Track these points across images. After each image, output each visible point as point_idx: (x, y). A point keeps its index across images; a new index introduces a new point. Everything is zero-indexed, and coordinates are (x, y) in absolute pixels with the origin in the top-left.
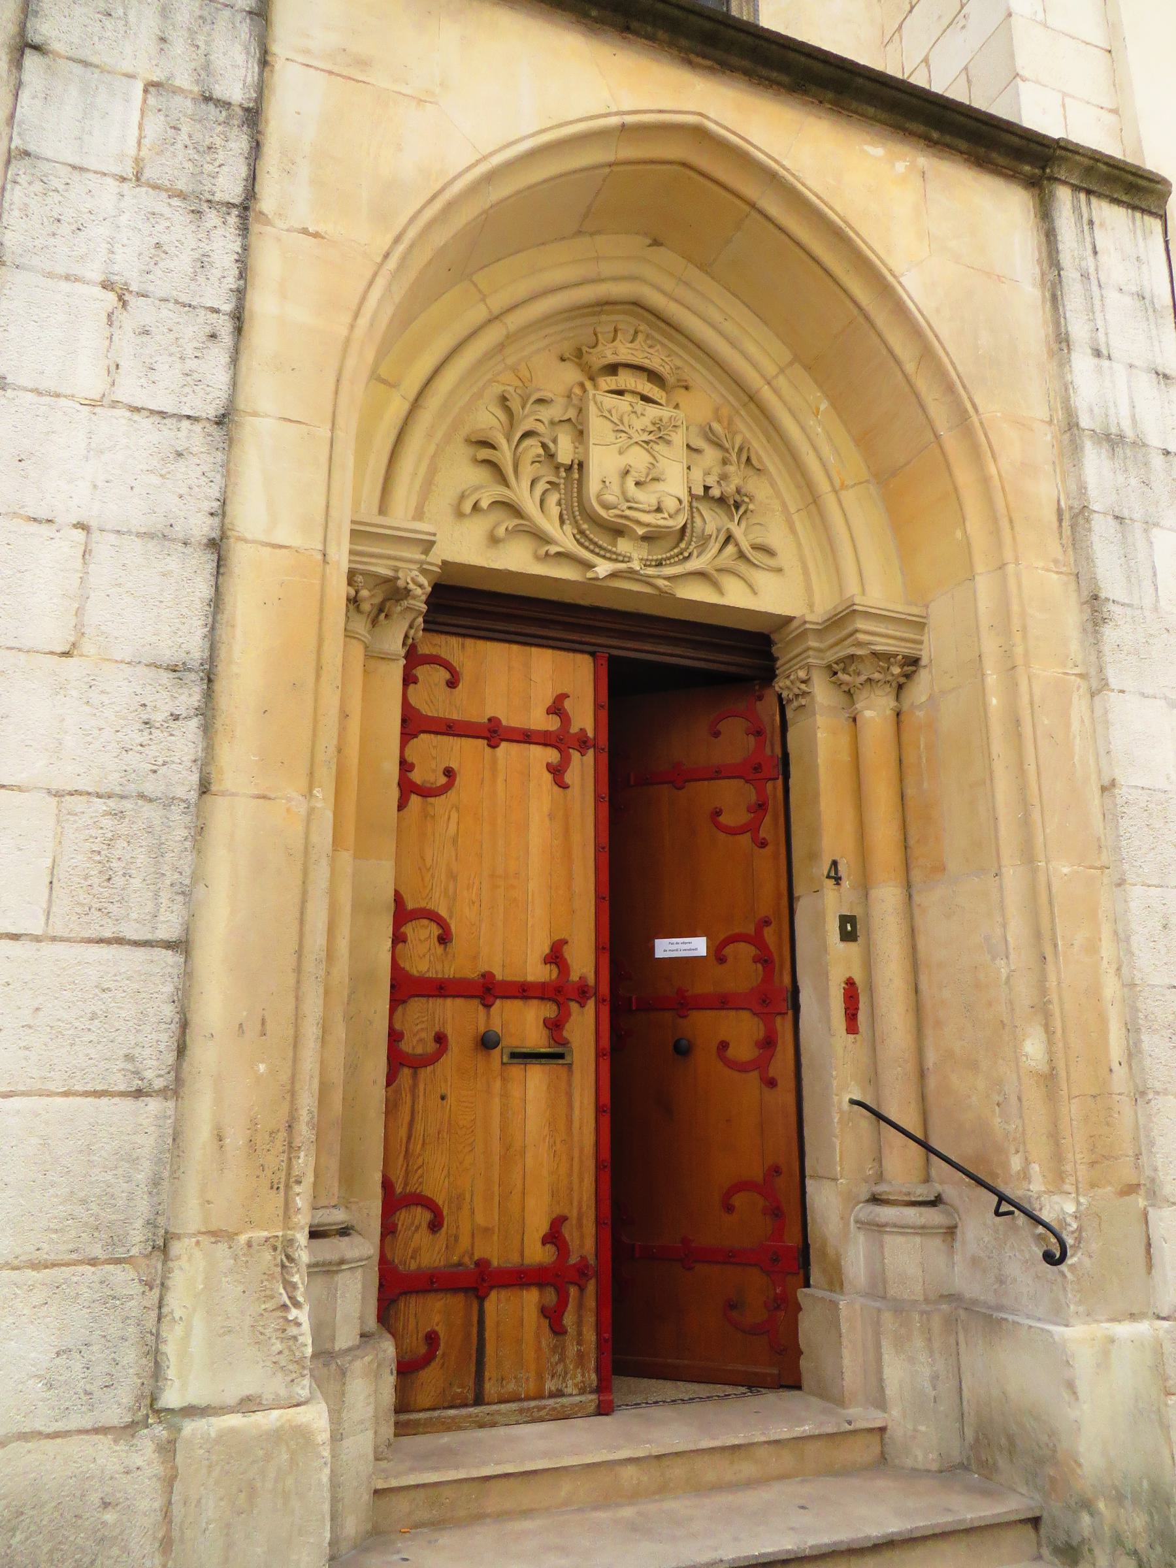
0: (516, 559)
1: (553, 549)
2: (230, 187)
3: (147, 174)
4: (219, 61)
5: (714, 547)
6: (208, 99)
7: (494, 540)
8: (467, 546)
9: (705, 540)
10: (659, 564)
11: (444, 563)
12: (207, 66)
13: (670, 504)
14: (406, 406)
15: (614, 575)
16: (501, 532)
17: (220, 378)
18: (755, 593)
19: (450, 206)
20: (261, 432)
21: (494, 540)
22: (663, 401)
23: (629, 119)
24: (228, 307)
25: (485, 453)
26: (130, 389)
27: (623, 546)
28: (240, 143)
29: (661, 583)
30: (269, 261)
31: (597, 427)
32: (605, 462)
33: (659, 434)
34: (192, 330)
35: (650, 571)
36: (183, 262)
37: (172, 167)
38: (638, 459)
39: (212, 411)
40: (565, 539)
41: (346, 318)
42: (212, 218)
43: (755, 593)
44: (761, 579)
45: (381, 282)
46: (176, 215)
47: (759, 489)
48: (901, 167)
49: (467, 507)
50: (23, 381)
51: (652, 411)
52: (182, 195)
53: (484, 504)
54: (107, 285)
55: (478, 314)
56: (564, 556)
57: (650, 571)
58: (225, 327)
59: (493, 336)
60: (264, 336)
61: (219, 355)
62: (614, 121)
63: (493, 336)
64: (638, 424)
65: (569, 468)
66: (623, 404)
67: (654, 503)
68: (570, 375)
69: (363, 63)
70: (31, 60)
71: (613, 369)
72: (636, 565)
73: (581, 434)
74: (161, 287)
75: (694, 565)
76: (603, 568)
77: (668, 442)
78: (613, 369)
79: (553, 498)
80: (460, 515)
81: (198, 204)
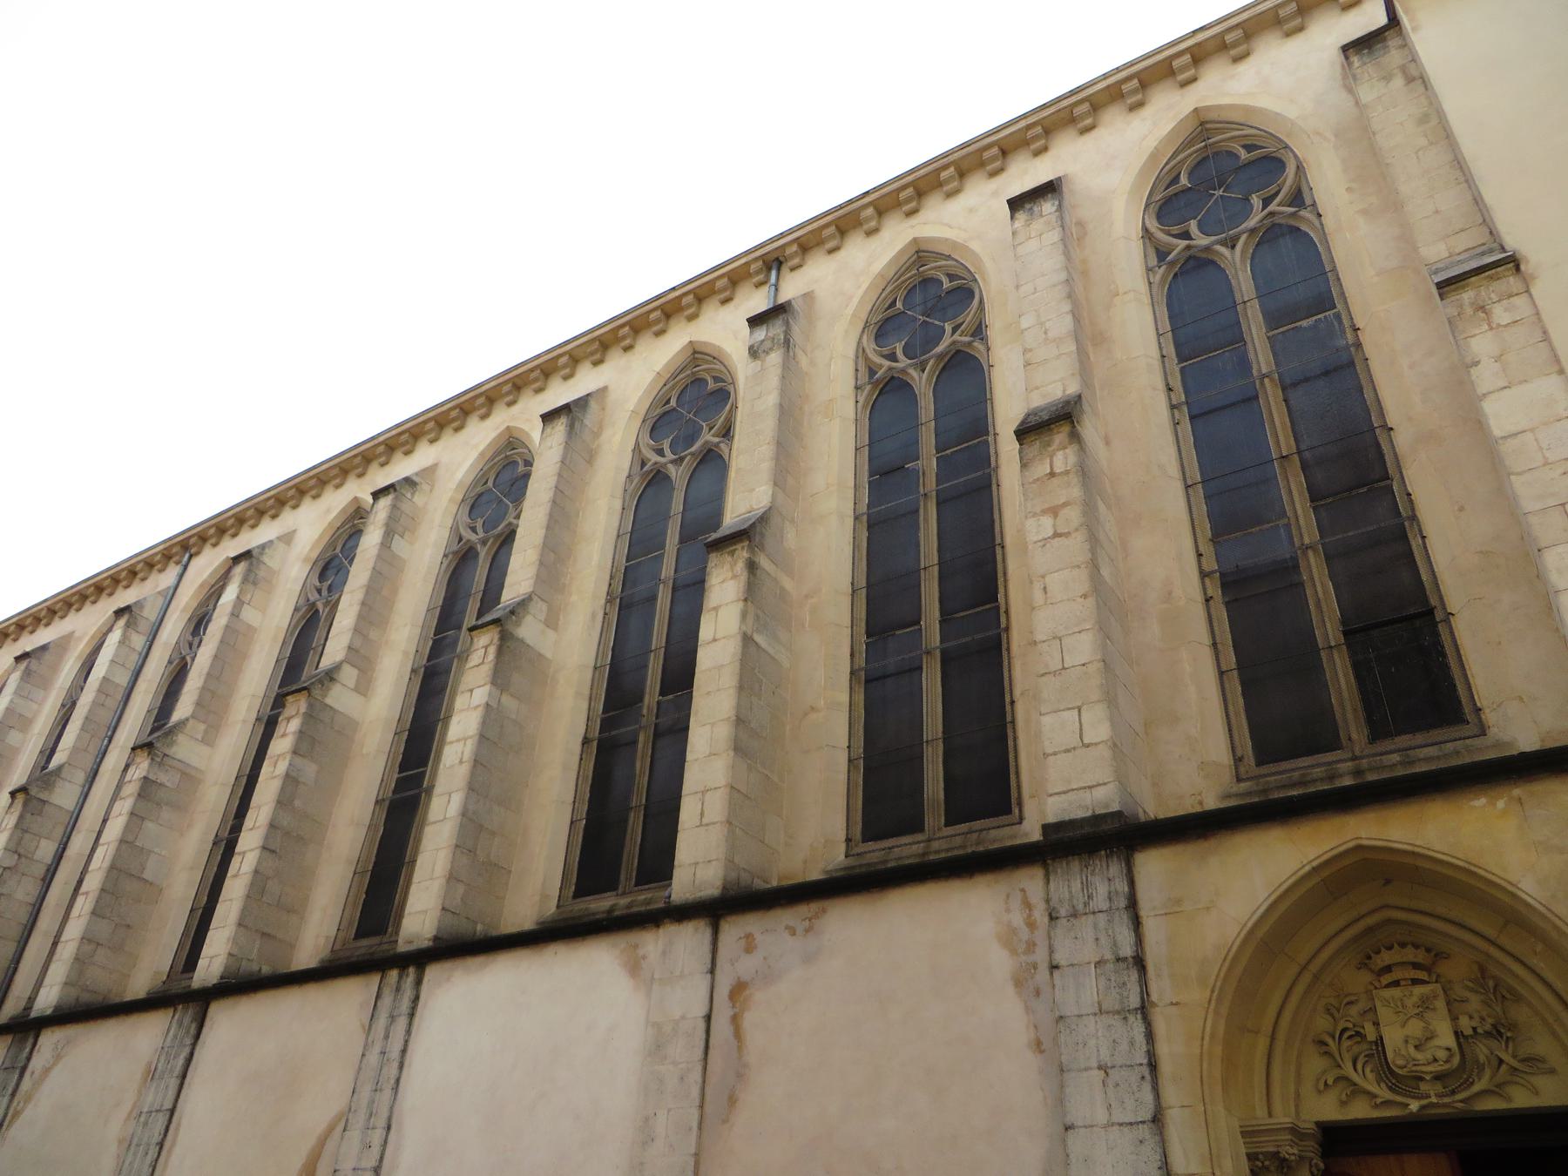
0: (1360, 1111)
1: (1379, 1101)
2: (1134, 1001)
3: (1104, 1007)
4: (1119, 938)
5: (1488, 1073)
6: (1118, 960)
7: (1343, 1103)
8: (1328, 1109)
9: (1481, 1068)
10: (1453, 1092)
11: (1318, 1124)
12: (1115, 944)
13: (1442, 1055)
14: (1268, 1041)
15: (1423, 1107)
16: (1344, 1097)
17: (1148, 1097)
18: (1537, 1093)
19: (1235, 958)
20: (1175, 1119)
21: (1343, 1103)
22: (1426, 978)
23: (1315, 864)
24: (1145, 1061)
25: (1324, 1049)
26: (1119, 1116)
27: (1424, 1087)
28: (1134, 975)
29: (1460, 1105)
30: (1160, 1027)
31: (1384, 1013)
32: (1393, 1038)
33: (1425, 1004)
34: (1134, 1077)
35: (1446, 1100)
36: (1124, 1046)
37: (1111, 1002)
38: (1415, 1028)
39: (1148, 1116)
40: (1384, 1093)
41: (1198, 1043)
42: (1131, 1018)
43: (1537, 1093)
44: (1541, 1081)
45: (1210, 1017)
46: (1115, 1021)
47: (1520, 1014)
48: (1501, 804)
49: (1322, 1086)
50: (1080, 1123)
51: (1419, 990)
52: (1118, 1012)
53: (1330, 1082)
54: (1100, 1068)
55: (1295, 969)
56: (1387, 1103)
57: (1446, 1100)
58: (1146, 1071)
59: (1307, 978)
60: (1166, 1067)
61: (1147, 1087)
62: (1307, 868)
63: (1307, 978)
64: (1409, 1002)
65: (1376, 1043)
66: (1395, 992)
67: (1430, 1057)
68: (1366, 977)
69: (1178, 902)
70: (1056, 973)
71: (1388, 969)
72: (1434, 1100)
73: (1376, 1024)
74: (1119, 1061)
75: (1476, 1088)
76: (1414, 1106)
77: (1434, 1009)
78: (1388, 969)
79: (1368, 1070)
80: (1320, 1092)
81: (1123, 1013)
